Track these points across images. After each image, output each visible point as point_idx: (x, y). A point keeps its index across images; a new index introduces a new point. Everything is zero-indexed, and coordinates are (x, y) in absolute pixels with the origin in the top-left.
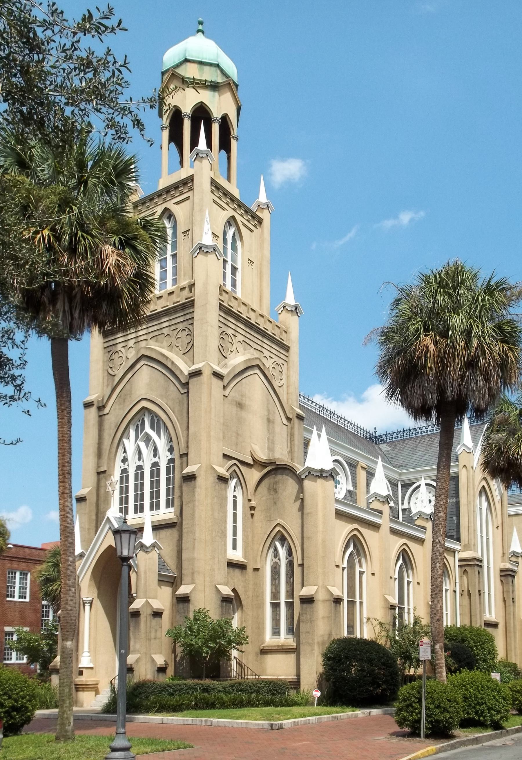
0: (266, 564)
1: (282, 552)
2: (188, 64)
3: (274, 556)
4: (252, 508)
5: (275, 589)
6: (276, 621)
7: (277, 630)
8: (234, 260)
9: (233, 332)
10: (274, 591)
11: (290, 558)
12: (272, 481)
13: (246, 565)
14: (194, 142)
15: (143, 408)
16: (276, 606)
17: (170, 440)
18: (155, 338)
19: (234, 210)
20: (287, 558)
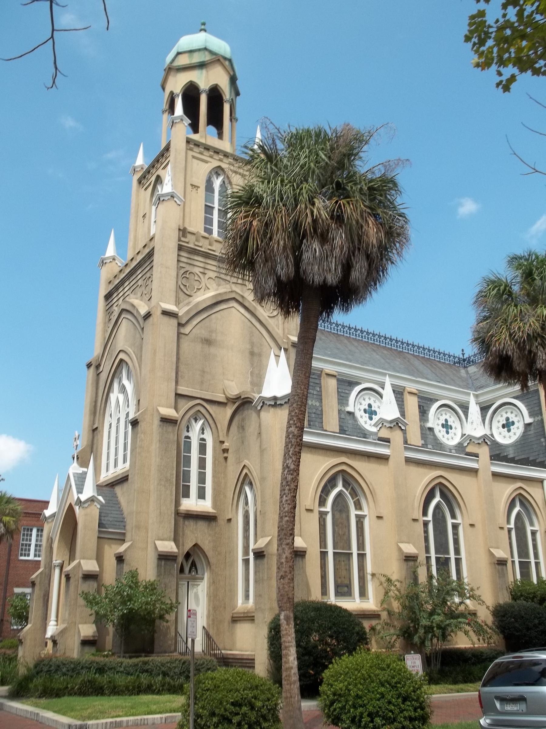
2: (180, 57)
4: (226, 451)
19: (220, 160)
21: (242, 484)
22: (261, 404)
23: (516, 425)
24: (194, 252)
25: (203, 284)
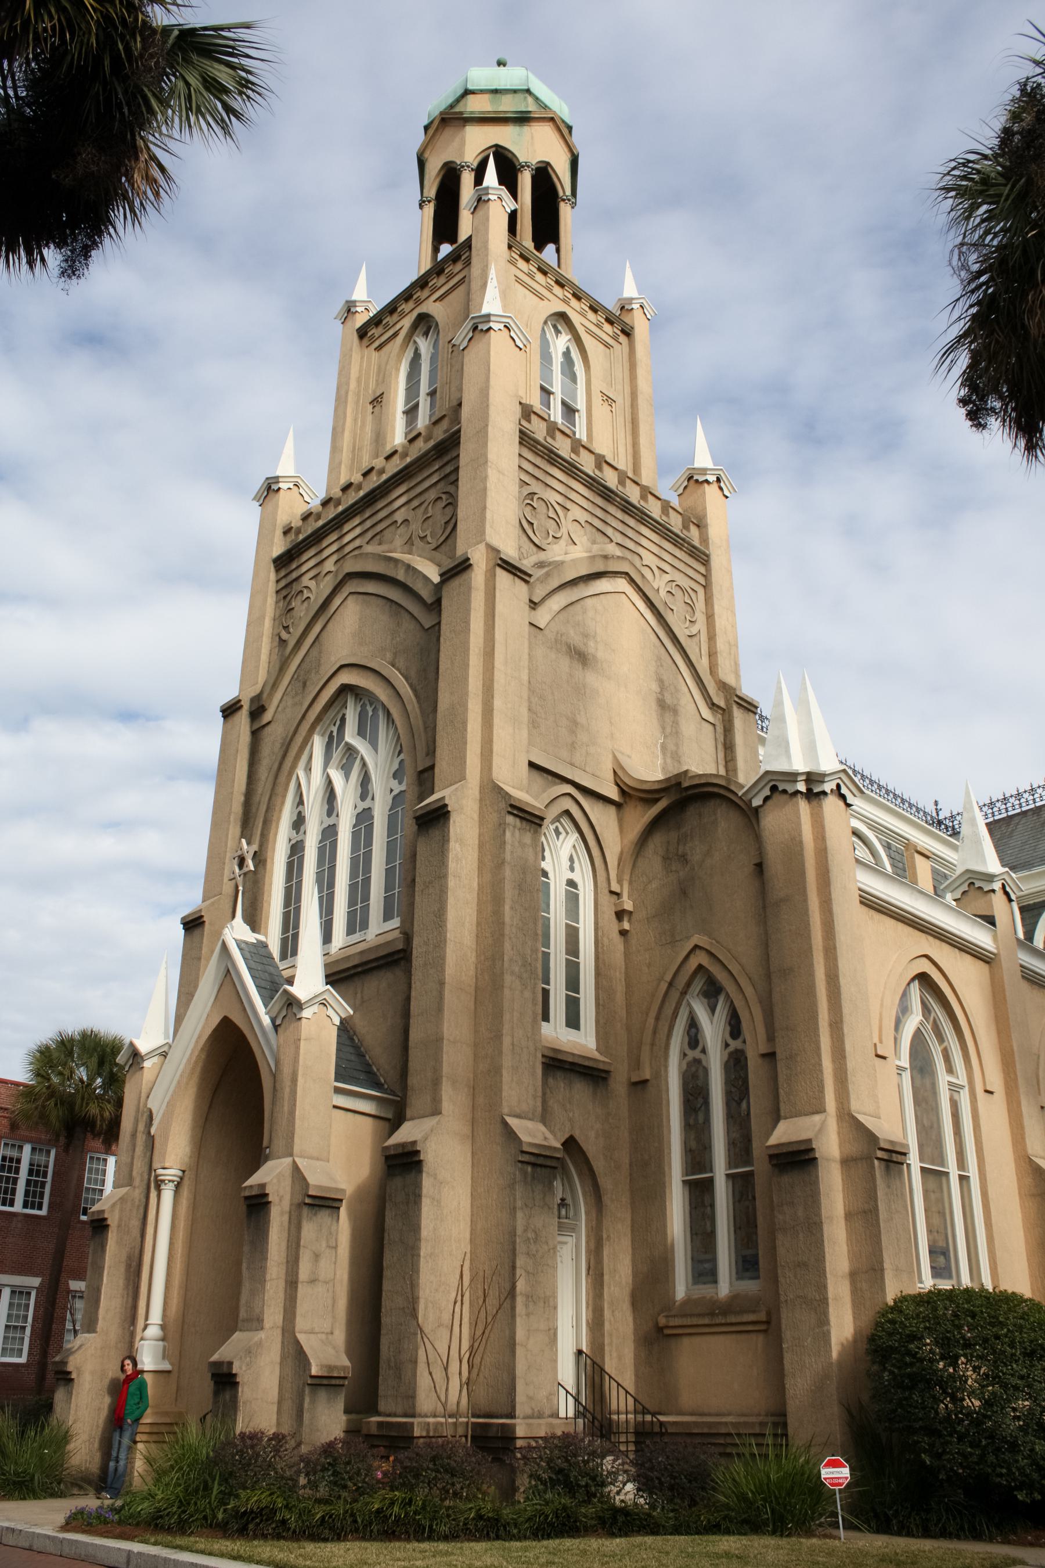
0: (666, 1067)
1: (713, 1030)
2: (470, 97)
3: (689, 1044)
7: (707, 1266)
9: (560, 499)
10: (693, 1145)
11: (734, 1044)
12: (673, 835)
13: (607, 1072)
15: (345, 689)
17: (399, 748)
18: (378, 537)
19: (565, 301)
20: (727, 1045)
21: (684, 993)
22: (767, 792)
24: (552, 457)
25: (564, 530)
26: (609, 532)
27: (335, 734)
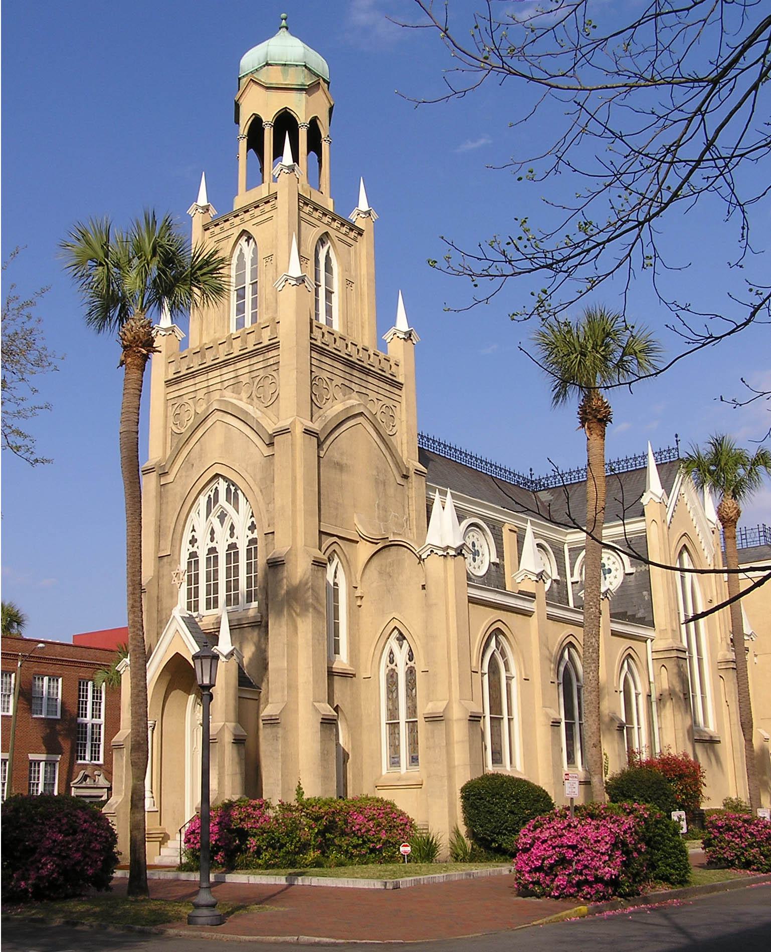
1: (401, 657)
5: (393, 704)
6: (395, 748)
8: (328, 282)
10: (391, 707)
14: (278, 152)
15: (217, 476)
16: (394, 726)
23: (613, 573)
26: (353, 386)
27: (212, 497)
